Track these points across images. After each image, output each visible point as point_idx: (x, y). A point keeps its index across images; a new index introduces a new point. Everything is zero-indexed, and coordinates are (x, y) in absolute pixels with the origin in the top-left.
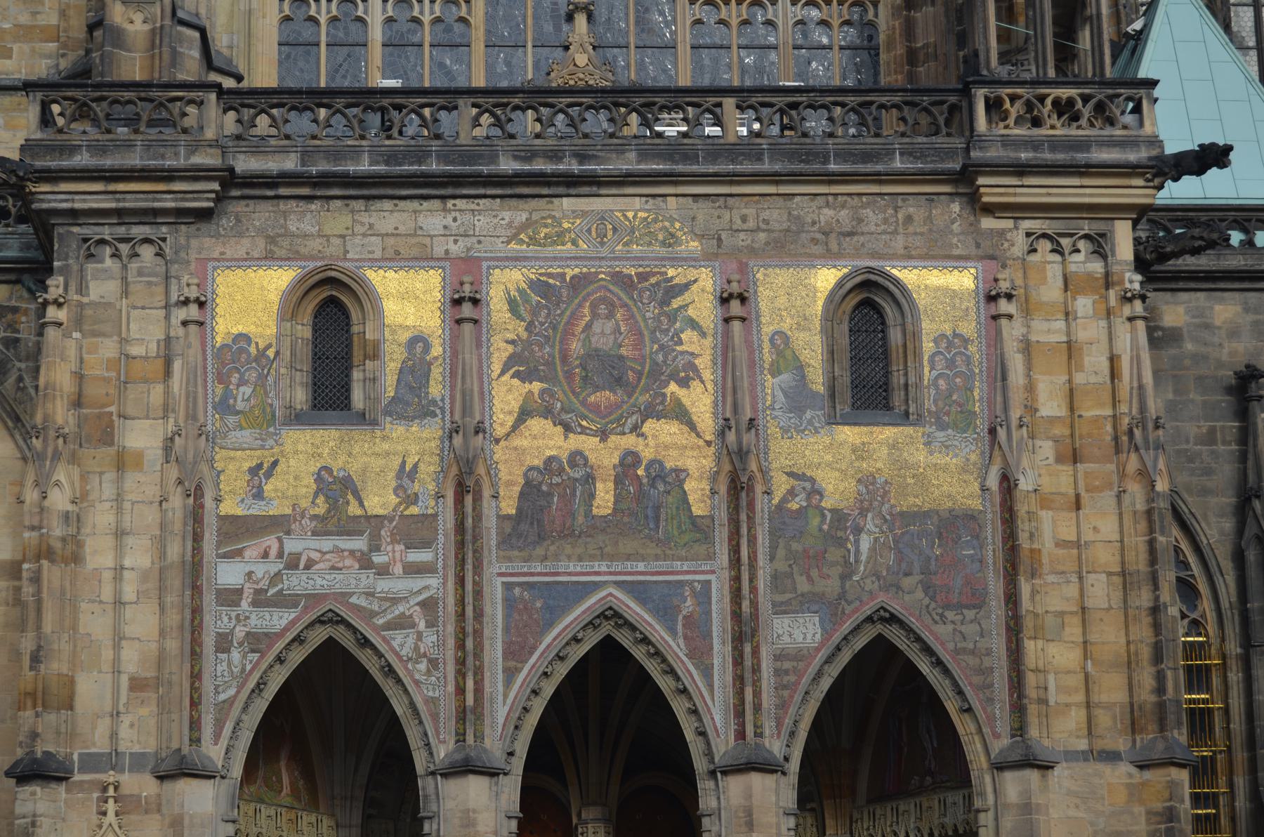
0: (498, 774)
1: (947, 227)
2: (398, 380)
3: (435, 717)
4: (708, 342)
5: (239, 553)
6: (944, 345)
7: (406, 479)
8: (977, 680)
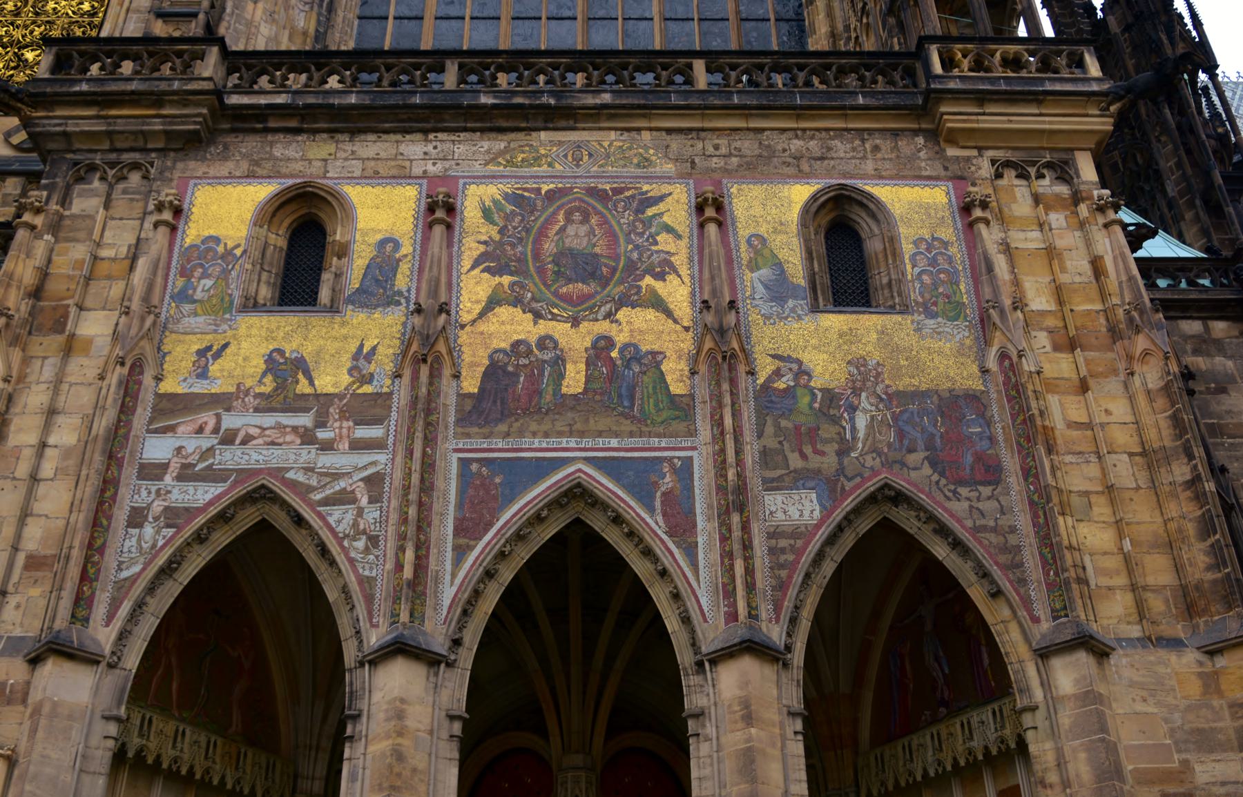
0: (439, 663)
1: (914, 154)
2: (365, 275)
3: (369, 599)
4: (683, 243)
5: (171, 429)
6: (924, 246)
7: (362, 362)
8: (1002, 559)
